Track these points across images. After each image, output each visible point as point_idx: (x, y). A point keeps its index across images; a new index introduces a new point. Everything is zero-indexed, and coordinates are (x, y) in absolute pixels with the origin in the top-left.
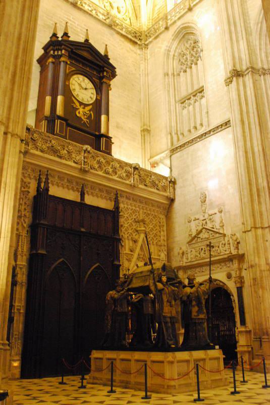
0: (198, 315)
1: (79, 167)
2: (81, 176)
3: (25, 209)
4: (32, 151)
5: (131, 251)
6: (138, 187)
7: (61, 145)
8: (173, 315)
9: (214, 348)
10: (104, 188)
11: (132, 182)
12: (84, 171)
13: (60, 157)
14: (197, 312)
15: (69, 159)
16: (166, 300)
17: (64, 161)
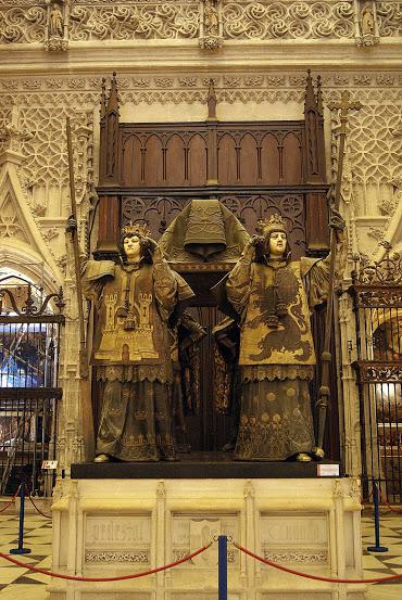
0: (269, 356)
1: (195, 42)
2: (206, 64)
3: (80, 168)
4: (72, 44)
5: (384, 213)
6: (376, 45)
7: (146, 9)
8: (132, 358)
9: (314, 475)
10: (281, 74)
11: (358, 35)
12: (210, 50)
13: (142, 35)
14: (264, 342)
15: (169, 33)
16: (113, 312)
17: (154, 42)
